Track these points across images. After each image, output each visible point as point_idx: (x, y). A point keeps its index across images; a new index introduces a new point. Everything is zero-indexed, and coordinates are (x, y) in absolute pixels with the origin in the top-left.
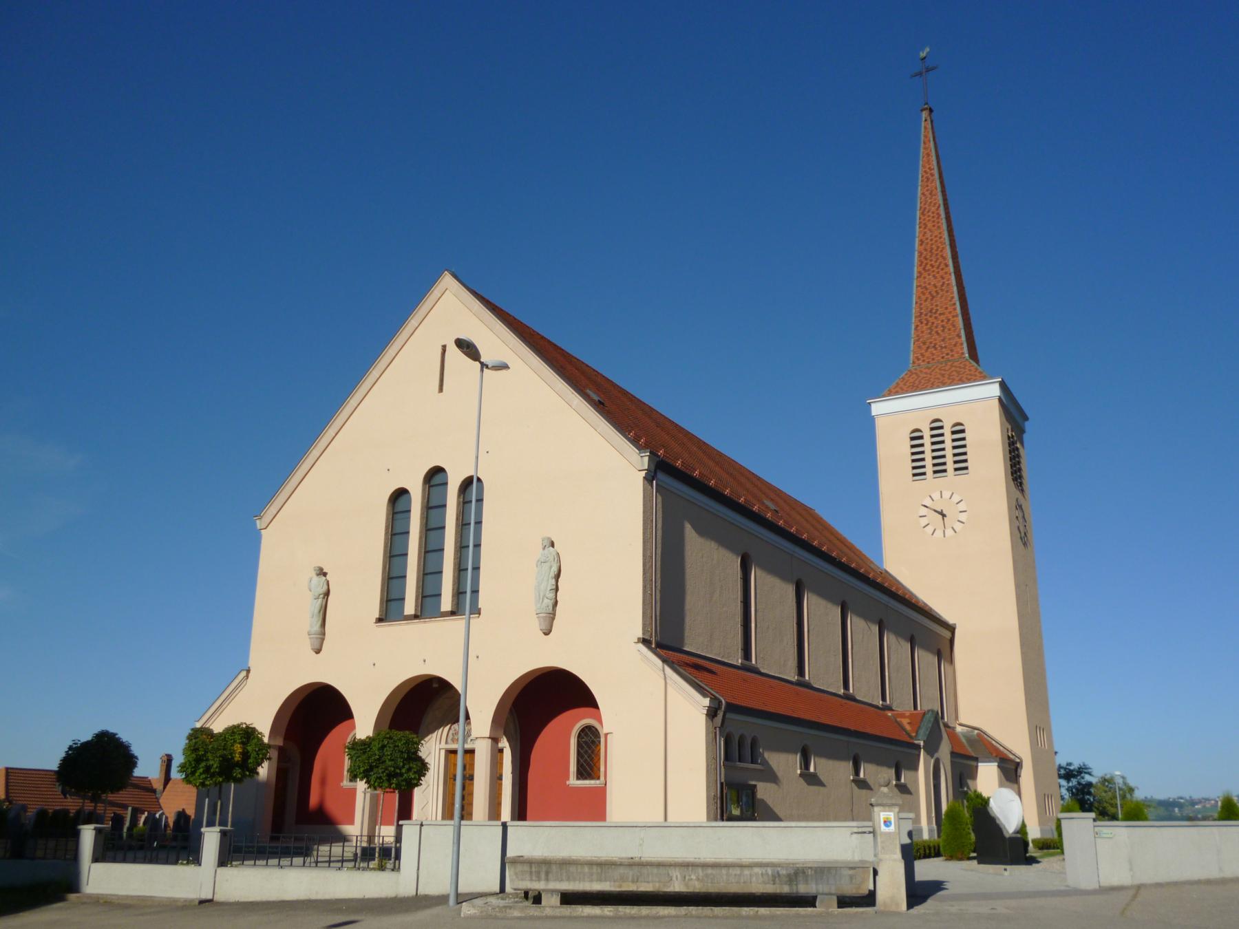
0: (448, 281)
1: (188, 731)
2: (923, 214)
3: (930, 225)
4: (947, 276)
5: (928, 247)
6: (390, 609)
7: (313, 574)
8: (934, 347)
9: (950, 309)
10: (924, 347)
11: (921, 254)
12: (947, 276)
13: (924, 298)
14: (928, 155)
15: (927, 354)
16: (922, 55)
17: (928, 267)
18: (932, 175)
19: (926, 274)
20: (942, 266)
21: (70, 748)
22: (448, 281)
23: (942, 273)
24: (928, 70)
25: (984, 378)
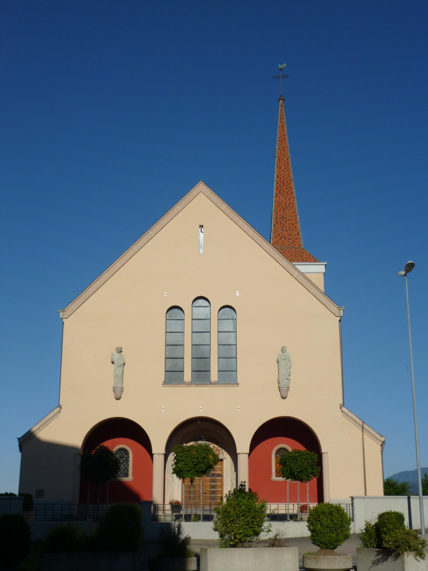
0: (201, 187)
1: (16, 444)
2: (279, 160)
3: (283, 167)
4: (292, 199)
5: (282, 180)
6: (173, 376)
7: (115, 352)
8: (284, 238)
9: (294, 218)
10: (279, 237)
11: (277, 183)
12: (292, 199)
13: (279, 209)
14: (283, 126)
15: (281, 241)
16: (280, 67)
17: (282, 192)
18: (285, 139)
19: (280, 195)
20: (290, 193)
21: (108, 447)
22: (201, 187)
23: (289, 196)
24: (284, 77)
25: (316, 261)
